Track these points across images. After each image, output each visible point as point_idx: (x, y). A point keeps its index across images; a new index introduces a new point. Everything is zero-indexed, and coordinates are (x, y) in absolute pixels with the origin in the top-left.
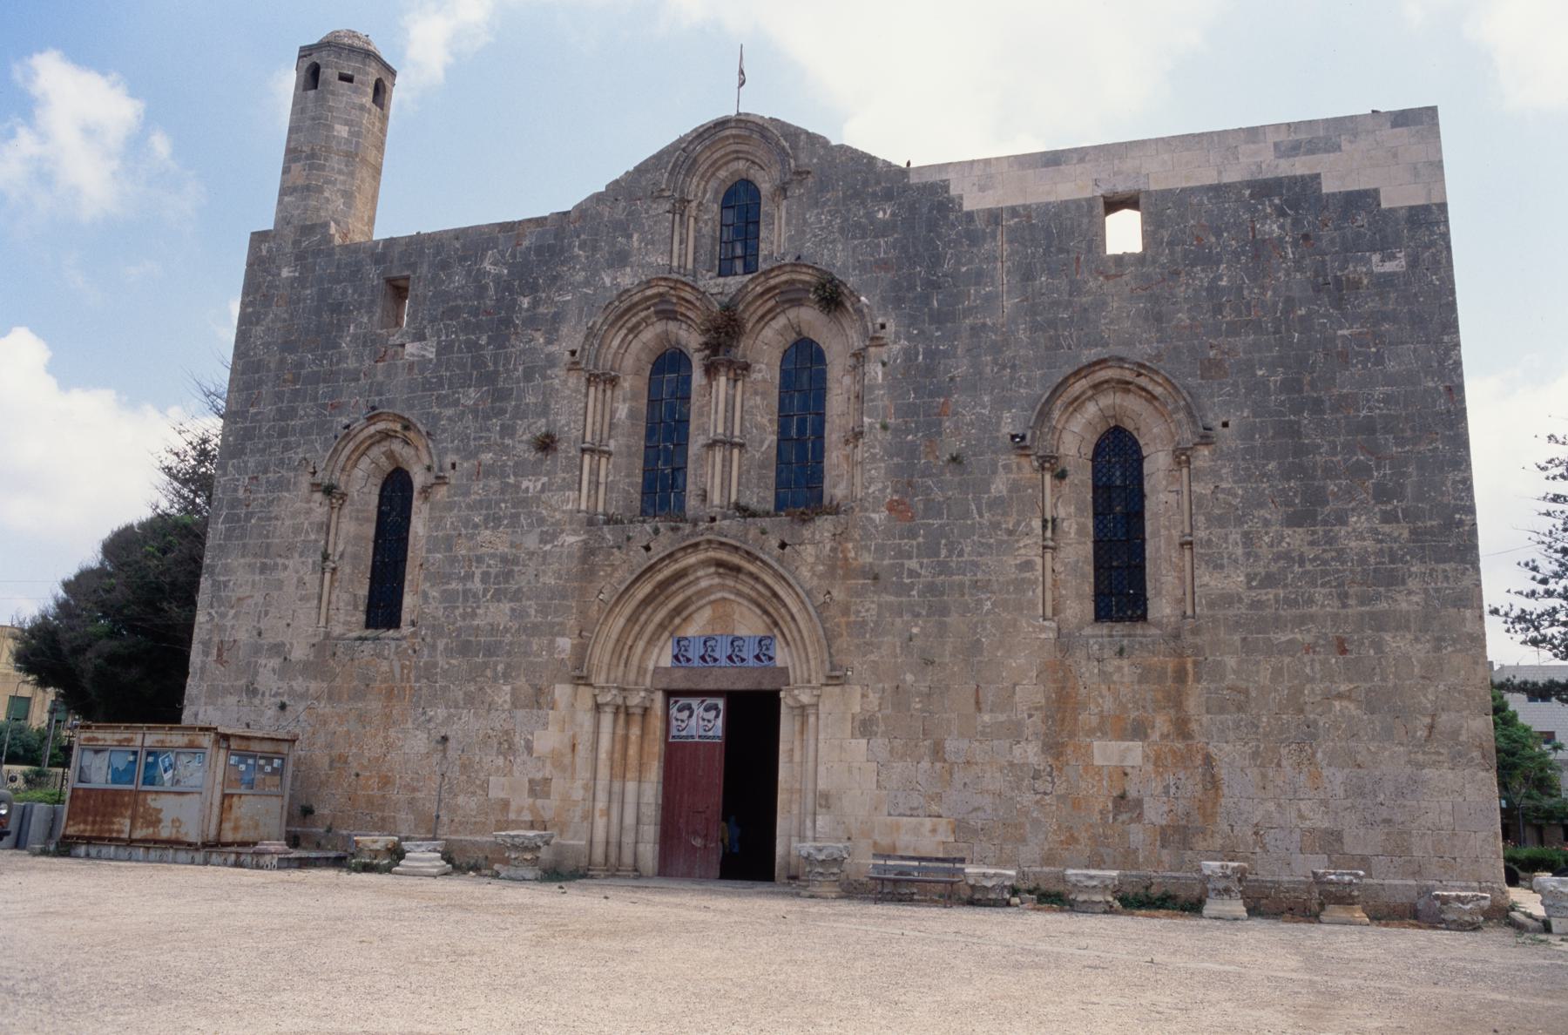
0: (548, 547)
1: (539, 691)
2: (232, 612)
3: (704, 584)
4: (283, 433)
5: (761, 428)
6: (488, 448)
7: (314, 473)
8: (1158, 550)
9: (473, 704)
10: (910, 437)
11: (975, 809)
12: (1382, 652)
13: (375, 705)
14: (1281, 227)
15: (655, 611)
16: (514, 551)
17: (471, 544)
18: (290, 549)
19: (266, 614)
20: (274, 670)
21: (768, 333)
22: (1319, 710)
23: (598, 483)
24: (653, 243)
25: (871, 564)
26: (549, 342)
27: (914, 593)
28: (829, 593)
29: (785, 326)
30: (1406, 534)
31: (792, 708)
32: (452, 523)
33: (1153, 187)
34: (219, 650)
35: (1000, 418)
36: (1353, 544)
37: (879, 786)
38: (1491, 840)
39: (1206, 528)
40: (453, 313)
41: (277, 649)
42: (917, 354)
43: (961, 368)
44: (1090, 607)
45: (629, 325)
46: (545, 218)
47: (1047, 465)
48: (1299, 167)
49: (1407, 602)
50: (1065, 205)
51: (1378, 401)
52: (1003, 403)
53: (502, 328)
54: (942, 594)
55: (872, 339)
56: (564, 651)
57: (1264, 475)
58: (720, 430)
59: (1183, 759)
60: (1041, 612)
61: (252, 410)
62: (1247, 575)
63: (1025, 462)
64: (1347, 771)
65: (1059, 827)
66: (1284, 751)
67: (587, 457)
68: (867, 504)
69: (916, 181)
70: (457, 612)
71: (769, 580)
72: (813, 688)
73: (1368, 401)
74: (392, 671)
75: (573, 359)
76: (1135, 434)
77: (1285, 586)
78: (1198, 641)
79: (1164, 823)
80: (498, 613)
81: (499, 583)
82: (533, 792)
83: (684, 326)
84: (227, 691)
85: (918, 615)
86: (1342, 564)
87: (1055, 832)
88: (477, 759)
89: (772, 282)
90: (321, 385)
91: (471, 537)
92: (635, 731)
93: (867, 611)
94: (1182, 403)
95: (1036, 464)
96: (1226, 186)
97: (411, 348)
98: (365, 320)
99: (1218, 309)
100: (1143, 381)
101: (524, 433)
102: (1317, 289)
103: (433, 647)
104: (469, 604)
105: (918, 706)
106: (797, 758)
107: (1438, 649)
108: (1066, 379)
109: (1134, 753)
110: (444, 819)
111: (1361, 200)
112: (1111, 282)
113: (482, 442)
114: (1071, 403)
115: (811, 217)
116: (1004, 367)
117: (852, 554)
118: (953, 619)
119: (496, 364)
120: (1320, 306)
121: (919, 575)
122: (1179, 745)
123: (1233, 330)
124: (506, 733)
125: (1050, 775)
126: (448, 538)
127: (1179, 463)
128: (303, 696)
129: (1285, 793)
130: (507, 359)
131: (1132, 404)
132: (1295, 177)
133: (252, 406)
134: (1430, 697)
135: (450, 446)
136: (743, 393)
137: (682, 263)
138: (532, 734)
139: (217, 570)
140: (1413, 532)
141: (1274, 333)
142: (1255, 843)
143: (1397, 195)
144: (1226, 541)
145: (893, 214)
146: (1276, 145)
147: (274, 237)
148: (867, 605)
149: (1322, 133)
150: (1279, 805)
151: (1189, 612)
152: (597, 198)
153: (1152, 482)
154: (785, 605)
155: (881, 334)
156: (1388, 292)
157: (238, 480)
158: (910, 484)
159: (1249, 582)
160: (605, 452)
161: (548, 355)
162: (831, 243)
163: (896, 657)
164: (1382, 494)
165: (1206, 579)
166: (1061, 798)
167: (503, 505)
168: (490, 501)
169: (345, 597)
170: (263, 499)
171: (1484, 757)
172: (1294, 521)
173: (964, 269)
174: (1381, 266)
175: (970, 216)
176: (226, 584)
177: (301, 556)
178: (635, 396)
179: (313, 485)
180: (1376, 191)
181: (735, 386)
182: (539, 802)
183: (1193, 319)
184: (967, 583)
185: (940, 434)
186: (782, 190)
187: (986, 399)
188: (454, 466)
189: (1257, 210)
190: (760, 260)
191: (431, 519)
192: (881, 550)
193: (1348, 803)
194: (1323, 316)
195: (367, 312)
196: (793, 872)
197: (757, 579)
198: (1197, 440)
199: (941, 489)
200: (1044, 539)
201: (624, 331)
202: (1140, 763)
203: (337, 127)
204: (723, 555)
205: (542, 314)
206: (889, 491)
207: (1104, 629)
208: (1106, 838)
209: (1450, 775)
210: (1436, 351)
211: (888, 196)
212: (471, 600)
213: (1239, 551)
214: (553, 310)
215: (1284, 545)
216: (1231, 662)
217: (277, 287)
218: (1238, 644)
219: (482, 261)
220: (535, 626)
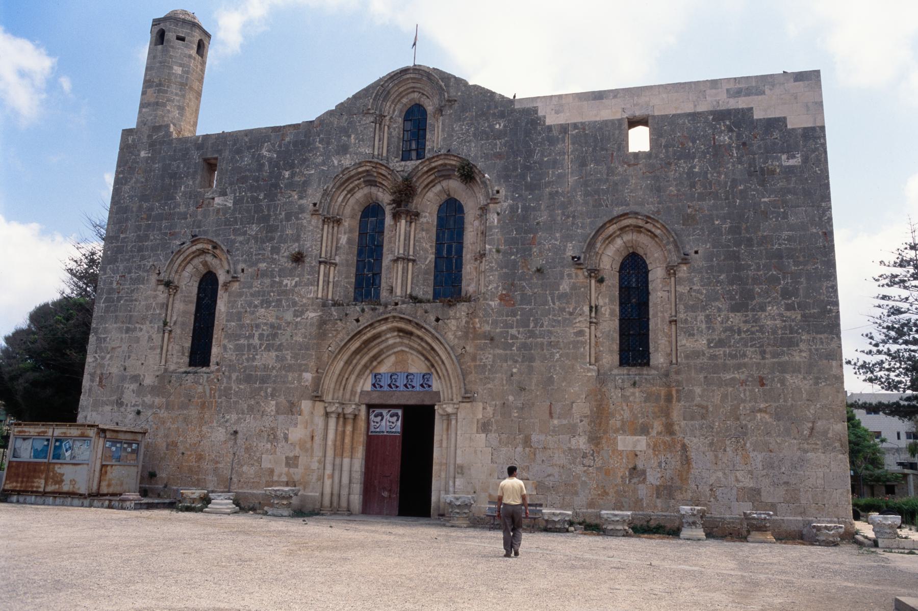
0: (299, 319)
1: (292, 405)
2: (108, 356)
3: (391, 342)
4: (140, 250)
5: (426, 250)
6: (264, 260)
7: (159, 274)
8: (657, 324)
9: (252, 412)
10: (513, 257)
11: (549, 475)
12: (785, 385)
13: (194, 412)
14: (730, 138)
15: (361, 357)
16: (278, 321)
17: (253, 317)
18: (144, 318)
19: (129, 358)
20: (133, 391)
21: (430, 195)
22: (749, 418)
23: (329, 282)
24: (363, 140)
26: (301, 198)
27: (514, 348)
28: (464, 348)
29: (440, 191)
30: (799, 317)
31: (442, 415)
32: (241, 304)
33: (656, 113)
34: (100, 379)
35: (565, 246)
36: (769, 323)
37: (492, 462)
38: (845, 494)
39: (684, 313)
40: (243, 180)
41: (135, 378)
42: (518, 208)
43: (543, 217)
44: (616, 358)
45: (349, 188)
46: (299, 125)
47: (593, 274)
48: (741, 103)
49: (799, 356)
50: (605, 123)
51: (784, 240)
52: (567, 238)
53: (273, 188)
54: (531, 349)
55: (491, 199)
56: (307, 380)
57: (718, 282)
58: (401, 251)
59: (669, 447)
60: (588, 360)
61: (122, 236)
62: (708, 340)
63: (580, 272)
64: (764, 454)
65: (597, 485)
66: (728, 442)
67: (322, 267)
68: (487, 296)
69: (519, 107)
70: (244, 357)
71: (429, 340)
72: (454, 404)
73: (778, 240)
74: (205, 392)
75: (315, 208)
76: (644, 257)
77: (730, 346)
78: (679, 378)
79: (658, 483)
80: (268, 358)
81: (269, 340)
82: (288, 465)
83: (381, 190)
84: (106, 403)
85: (516, 361)
86: (762, 334)
87: (595, 489)
88: (255, 444)
89: (433, 165)
90: (164, 222)
91: (253, 313)
92: (349, 428)
93: (487, 359)
94: (672, 239)
95: (586, 274)
96: (699, 113)
97: (218, 200)
98: (191, 183)
99: (693, 185)
100: (649, 226)
101: (285, 252)
102: (750, 174)
103: (230, 378)
104: (252, 352)
105: (516, 415)
106: (444, 445)
107: (816, 383)
108: (605, 224)
109: (641, 443)
110: (235, 480)
111: (776, 123)
112: (631, 168)
113: (260, 257)
114: (607, 239)
115: (456, 127)
116: (568, 217)
117: (478, 325)
118: (537, 364)
119: (269, 210)
120: (752, 184)
121: (517, 338)
122: (668, 438)
123: (702, 197)
124: (272, 429)
125: (592, 455)
126: (239, 313)
127: (669, 274)
128: (151, 406)
129: (728, 466)
130: (276, 207)
131: (643, 239)
132: (738, 109)
133: (122, 233)
134: (812, 411)
135: (241, 258)
136: (415, 230)
137: (380, 153)
138: (288, 430)
139: (100, 331)
140: (803, 316)
141: (725, 199)
142: (711, 495)
143: (797, 121)
144: (696, 320)
145: (505, 126)
146: (728, 90)
147: (136, 133)
148: (487, 355)
149: (754, 84)
150: (725, 474)
151: (674, 361)
152: (330, 113)
153: (654, 285)
154: (438, 355)
155: (497, 196)
156: (791, 177)
157: (113, 277)
158: (512, 284)
159: (709, 344)
160: (333, 264)
161: (300, 206)
162: (468, 142)
163: (503, 386)
164: (786, 294)
165: (684, 342)
166: (599, 469)
167: (272, 294)
168: (264, 291)
169: (177, 347)
170: (128, 288)
171: (842, 446)
172: (734, 309)
173: (546, 159)
174: (786, 161)
175: (550, 128)
176: (105, 339)
177: (150, 323)
178: (351, 231)
179: (158, 281)
180: (785, 118)
181: (410, 226)
182: (292, 470)
183: (679, 191)
184: (546, 343)
185: (530, 255)
186: (440, 111)
187: (558, 235)
188: (243, 270)
189: (716, 128)
190: (426, 152)
191: (229, 302)
192: (495, 323)
193: (764, 472)
194: (754, 190)
195: (192, 178)
196: (441, 512)
197: (422, 339)
198: (680, 261)
199: (531, 288)
200: (591, 318)
201: (345, 192)
202: (645, 449)
203: (175, 68)
204: (402, 325)
205: (297, 181)
206: (500, 288)
207: (625, 370)
208: (625, 492)
209: (823, 457)
210: (818, 211)
211: (502, 115)
212: (252, 350)
213: (704, 326)
214: (303, 179)
215: (729, 322)
216: (698, 390)
217: (138, 163)
218: (702, 380)
219: (261, 150)
220: (290, 366)
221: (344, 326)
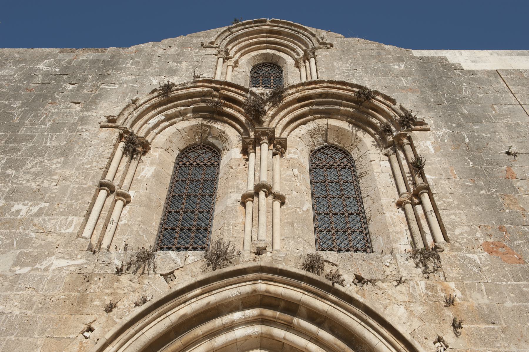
0: (25, 270)
25: (488, 306)
45: (169, 112)
67: (103, 193)
178: (161, 163)
201: (161, 117)
221: (137, 286)
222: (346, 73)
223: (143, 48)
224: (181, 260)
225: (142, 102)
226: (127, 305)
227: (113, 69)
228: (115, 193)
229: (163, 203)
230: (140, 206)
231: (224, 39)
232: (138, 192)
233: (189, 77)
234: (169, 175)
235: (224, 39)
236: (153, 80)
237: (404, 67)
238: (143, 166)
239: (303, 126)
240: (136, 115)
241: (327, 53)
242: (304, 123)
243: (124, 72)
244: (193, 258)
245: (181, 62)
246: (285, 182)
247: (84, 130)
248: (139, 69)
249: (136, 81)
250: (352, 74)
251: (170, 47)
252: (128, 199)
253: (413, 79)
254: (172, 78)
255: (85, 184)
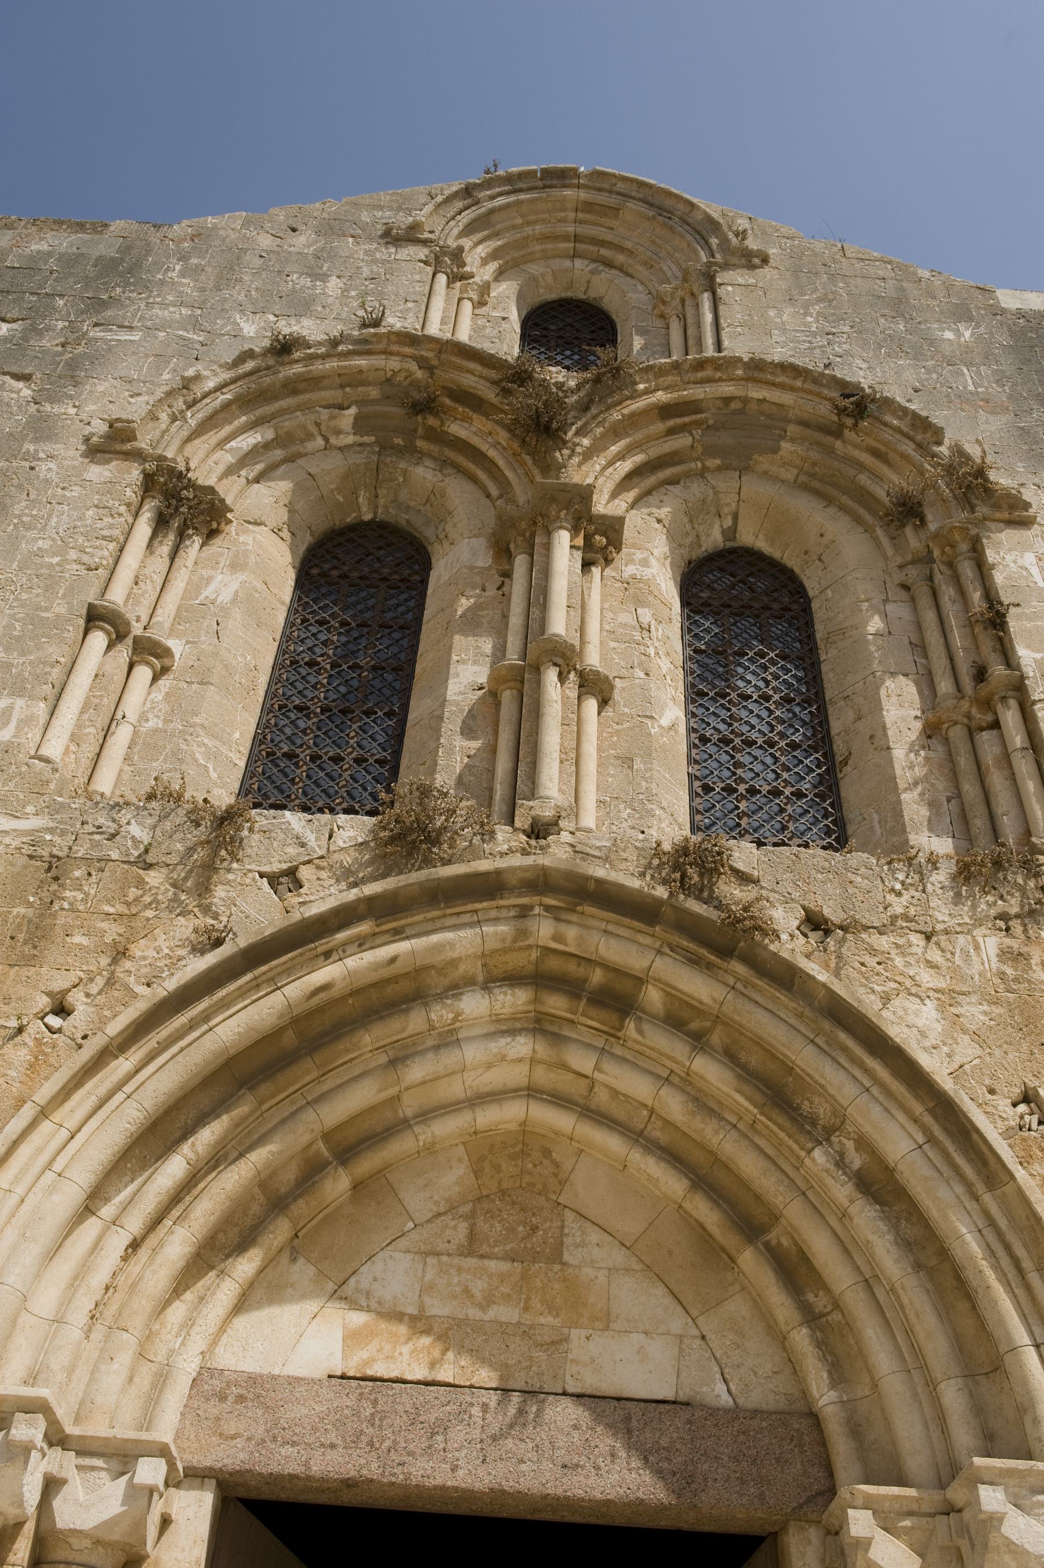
67: (98, 640)
222: (804, 341)
223: (215, 228)
224: (317, 839)
225: (211, 384)
226: (166, 951)
227: (127, 284)
228: (129, 641)
229: (263, 680)
230: (198, 683)
231: (453, 218)
232: (193, 643)
233: (344, 321)
234: (283, 603)
235: (453, 218)
236: (242, 325)
237: (972, 335)
238: (210, 572)
239: (671, 488)
240: (193, 423)
241: (751, 281)
242: (673, 481)
243: (158, 296)
244: (351, 833)
245: (324, 278)
246: (613, 644)
247: (42, 455)
248: (202, 290)
249: (195, 325)
250: (821, 347)
251: (294, 230)
252: (167, 661)
253: (994, 372)
254: (299, 322)
255: (47, 609)
